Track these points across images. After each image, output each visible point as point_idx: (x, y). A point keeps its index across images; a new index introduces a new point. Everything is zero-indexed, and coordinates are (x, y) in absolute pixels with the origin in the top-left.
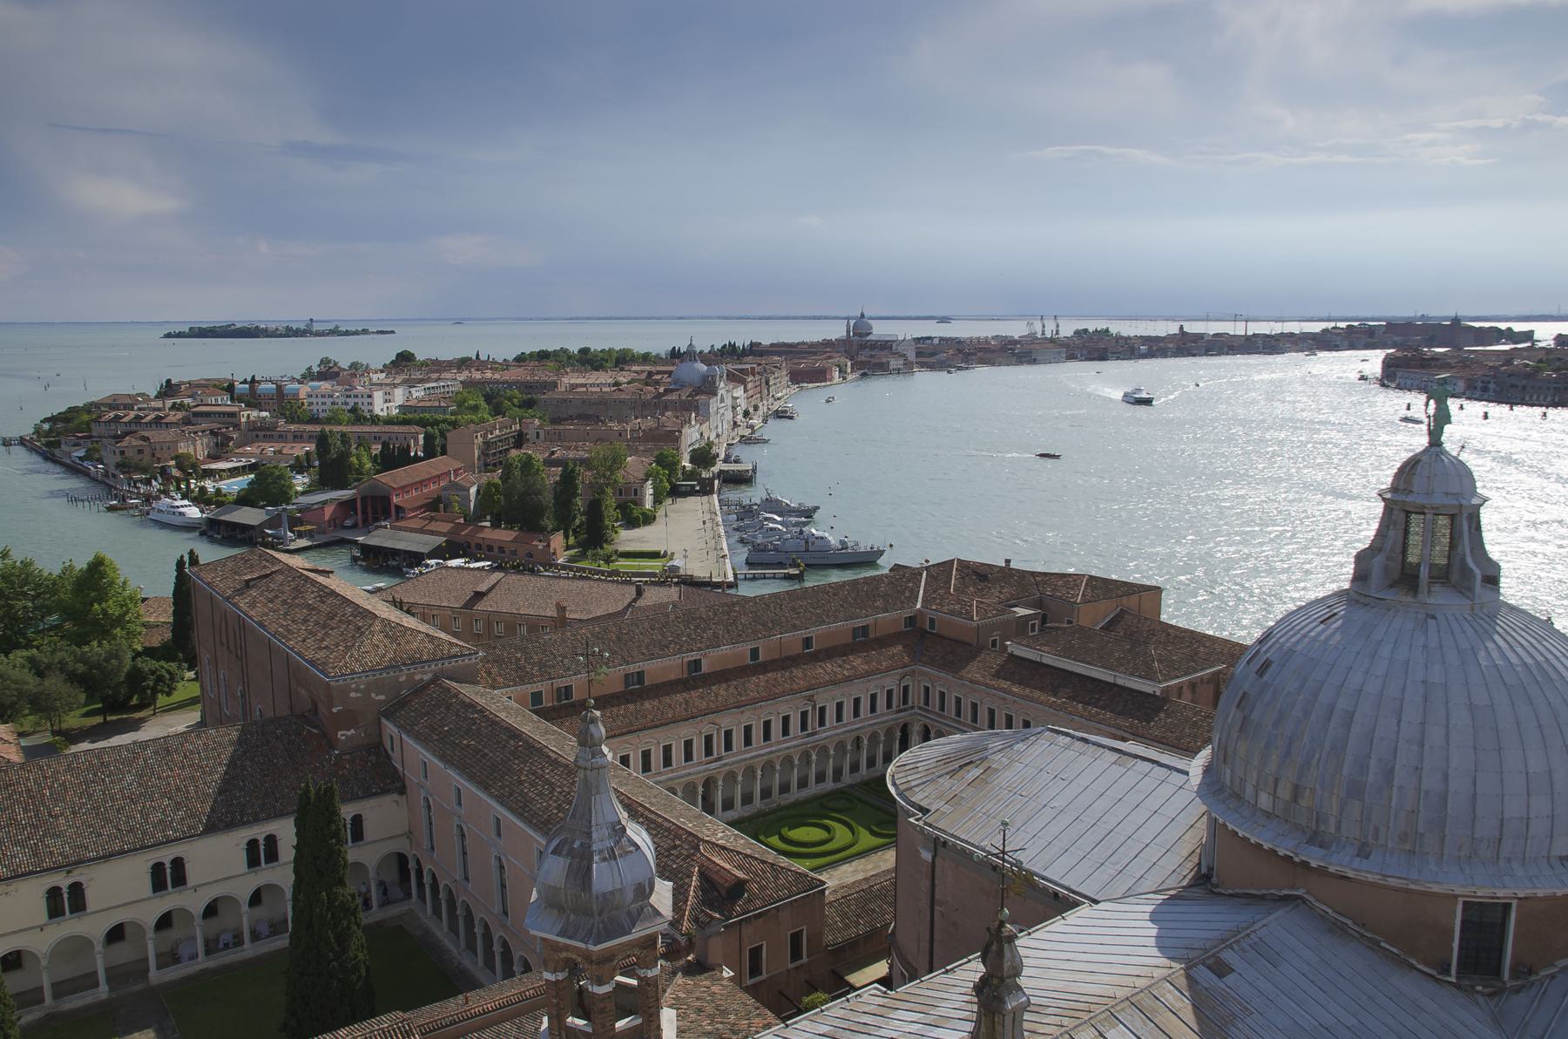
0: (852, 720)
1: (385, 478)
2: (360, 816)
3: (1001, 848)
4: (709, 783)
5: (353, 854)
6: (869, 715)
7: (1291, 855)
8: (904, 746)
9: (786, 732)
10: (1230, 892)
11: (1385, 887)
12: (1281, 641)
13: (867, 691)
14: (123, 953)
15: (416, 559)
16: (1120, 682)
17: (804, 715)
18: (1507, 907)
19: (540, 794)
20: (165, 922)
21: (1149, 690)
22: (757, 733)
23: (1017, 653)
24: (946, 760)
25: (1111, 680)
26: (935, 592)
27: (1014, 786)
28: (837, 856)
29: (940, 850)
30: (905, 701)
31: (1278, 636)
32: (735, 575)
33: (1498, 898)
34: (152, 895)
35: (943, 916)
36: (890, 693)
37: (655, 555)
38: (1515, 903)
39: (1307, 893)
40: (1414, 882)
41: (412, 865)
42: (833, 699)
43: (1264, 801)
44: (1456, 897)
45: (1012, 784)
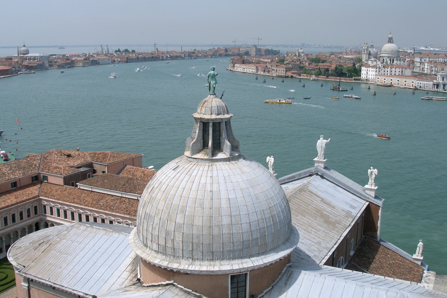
0: (12, 224)
6: (4, 227)
7: (167, 268)
10: (148, 285)
12: (158, 179)
13: (18, 211)
18: (246, 274)
24: (33, 243)
25: (120, 195)
26: (46, 164)
27: (62, 251)
28: (7, 286)
29: (30, 282)
30: (36, 213)
31: (157, 177)
33: (242, 272)
38: (248, 273)
39: (174, 282)
40: (212, 271)
43: (155, 247)
44: (228, 274)
45: (61, 250)
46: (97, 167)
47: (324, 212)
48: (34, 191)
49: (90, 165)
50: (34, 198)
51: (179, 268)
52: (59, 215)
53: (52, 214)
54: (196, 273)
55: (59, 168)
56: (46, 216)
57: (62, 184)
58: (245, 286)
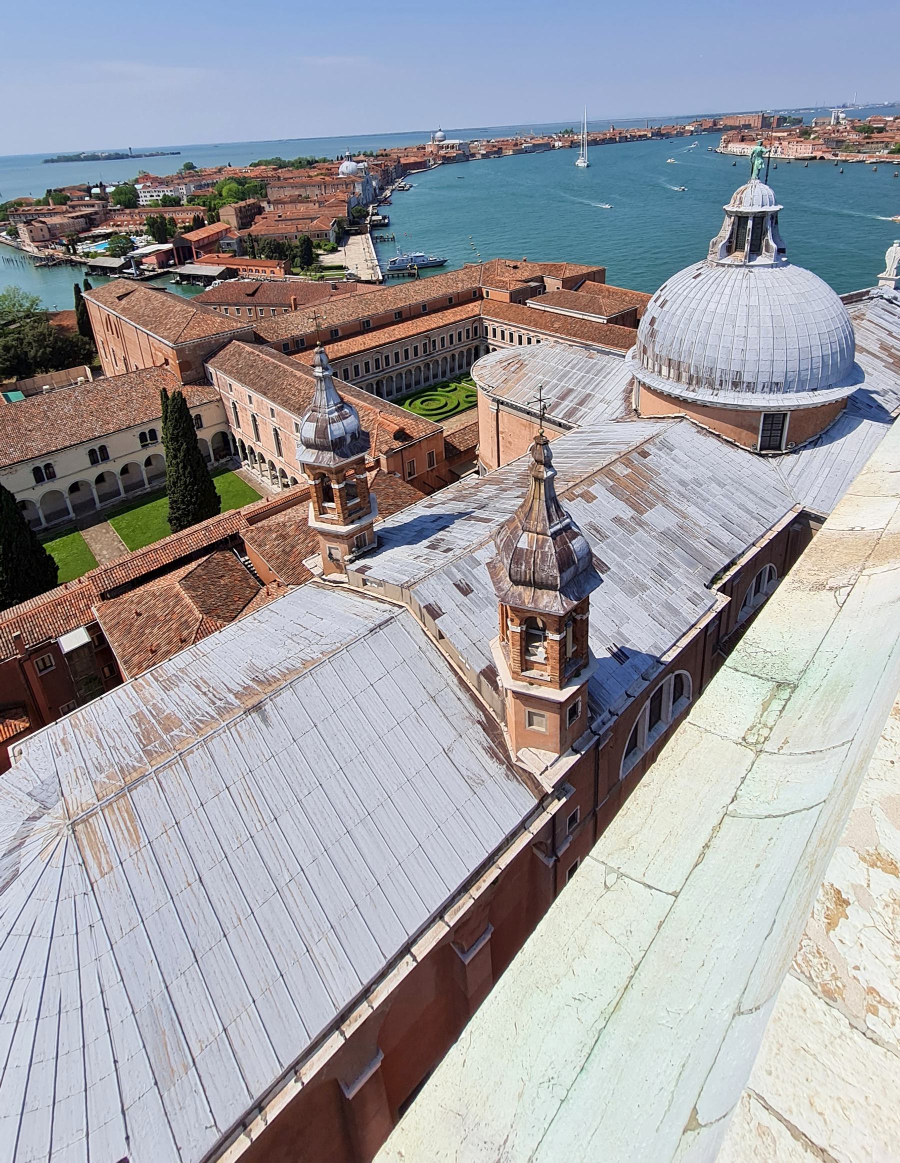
1: (186, 236)
2: (199, 415)
3: (538, 397)
4: (379, 383)
5: (200, 434)
8: (477, 357)
9: (416, 354)
11: (725, 410)
14: (80, 497)
15: (209, 280)
16: (586, 317)
17: (425, 344)
19: (294, 395)
20: (100, 479)
21: (601, 321)
22: (402, 356)
23: (532, 306)
25: (581, 317)
30: (476, 335)
32: (383, 276)
34: (90, 465)
35: (503, 438)
36: (468, 330)
37: (341, 268)
41: (230, 437)
42: (439, 335)
46: (548, 281)
47: (893, 351)
48: (473, 308)
49: (541, 279)
50: (474, 316)
51: (696, 398)
52: (503, 338)
53: (495, 336)
54: (718, 406)
55: (504, 282)
56: (487, 339)
57: (508, 301)
58: (782, 430)
